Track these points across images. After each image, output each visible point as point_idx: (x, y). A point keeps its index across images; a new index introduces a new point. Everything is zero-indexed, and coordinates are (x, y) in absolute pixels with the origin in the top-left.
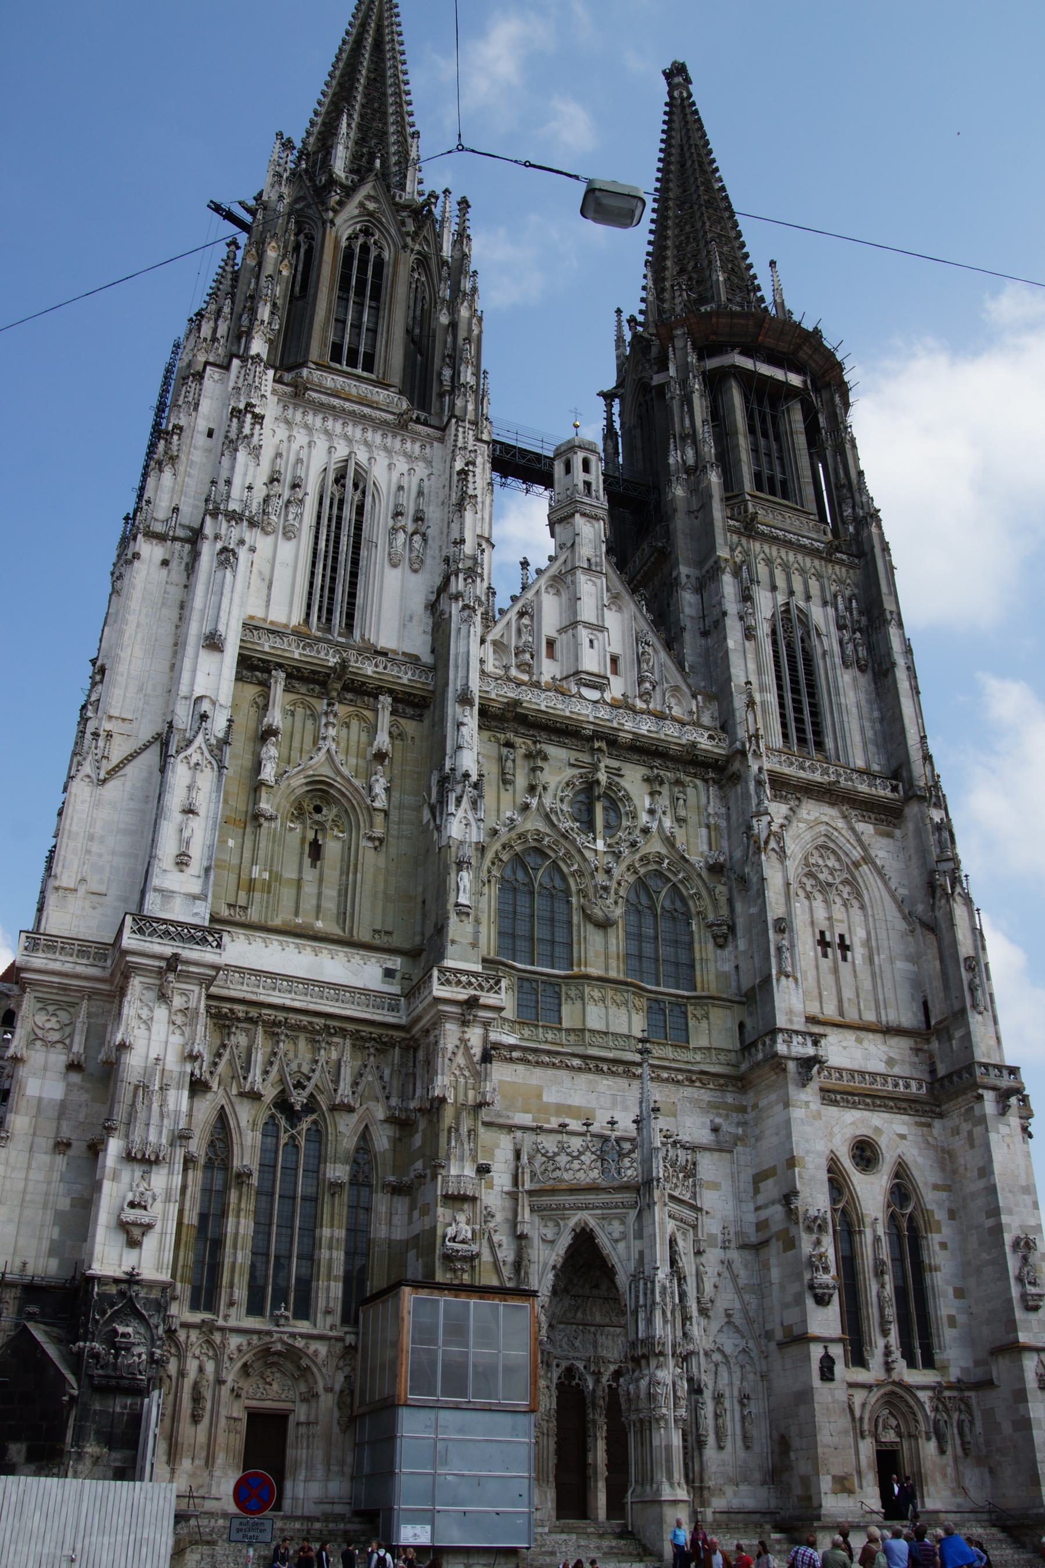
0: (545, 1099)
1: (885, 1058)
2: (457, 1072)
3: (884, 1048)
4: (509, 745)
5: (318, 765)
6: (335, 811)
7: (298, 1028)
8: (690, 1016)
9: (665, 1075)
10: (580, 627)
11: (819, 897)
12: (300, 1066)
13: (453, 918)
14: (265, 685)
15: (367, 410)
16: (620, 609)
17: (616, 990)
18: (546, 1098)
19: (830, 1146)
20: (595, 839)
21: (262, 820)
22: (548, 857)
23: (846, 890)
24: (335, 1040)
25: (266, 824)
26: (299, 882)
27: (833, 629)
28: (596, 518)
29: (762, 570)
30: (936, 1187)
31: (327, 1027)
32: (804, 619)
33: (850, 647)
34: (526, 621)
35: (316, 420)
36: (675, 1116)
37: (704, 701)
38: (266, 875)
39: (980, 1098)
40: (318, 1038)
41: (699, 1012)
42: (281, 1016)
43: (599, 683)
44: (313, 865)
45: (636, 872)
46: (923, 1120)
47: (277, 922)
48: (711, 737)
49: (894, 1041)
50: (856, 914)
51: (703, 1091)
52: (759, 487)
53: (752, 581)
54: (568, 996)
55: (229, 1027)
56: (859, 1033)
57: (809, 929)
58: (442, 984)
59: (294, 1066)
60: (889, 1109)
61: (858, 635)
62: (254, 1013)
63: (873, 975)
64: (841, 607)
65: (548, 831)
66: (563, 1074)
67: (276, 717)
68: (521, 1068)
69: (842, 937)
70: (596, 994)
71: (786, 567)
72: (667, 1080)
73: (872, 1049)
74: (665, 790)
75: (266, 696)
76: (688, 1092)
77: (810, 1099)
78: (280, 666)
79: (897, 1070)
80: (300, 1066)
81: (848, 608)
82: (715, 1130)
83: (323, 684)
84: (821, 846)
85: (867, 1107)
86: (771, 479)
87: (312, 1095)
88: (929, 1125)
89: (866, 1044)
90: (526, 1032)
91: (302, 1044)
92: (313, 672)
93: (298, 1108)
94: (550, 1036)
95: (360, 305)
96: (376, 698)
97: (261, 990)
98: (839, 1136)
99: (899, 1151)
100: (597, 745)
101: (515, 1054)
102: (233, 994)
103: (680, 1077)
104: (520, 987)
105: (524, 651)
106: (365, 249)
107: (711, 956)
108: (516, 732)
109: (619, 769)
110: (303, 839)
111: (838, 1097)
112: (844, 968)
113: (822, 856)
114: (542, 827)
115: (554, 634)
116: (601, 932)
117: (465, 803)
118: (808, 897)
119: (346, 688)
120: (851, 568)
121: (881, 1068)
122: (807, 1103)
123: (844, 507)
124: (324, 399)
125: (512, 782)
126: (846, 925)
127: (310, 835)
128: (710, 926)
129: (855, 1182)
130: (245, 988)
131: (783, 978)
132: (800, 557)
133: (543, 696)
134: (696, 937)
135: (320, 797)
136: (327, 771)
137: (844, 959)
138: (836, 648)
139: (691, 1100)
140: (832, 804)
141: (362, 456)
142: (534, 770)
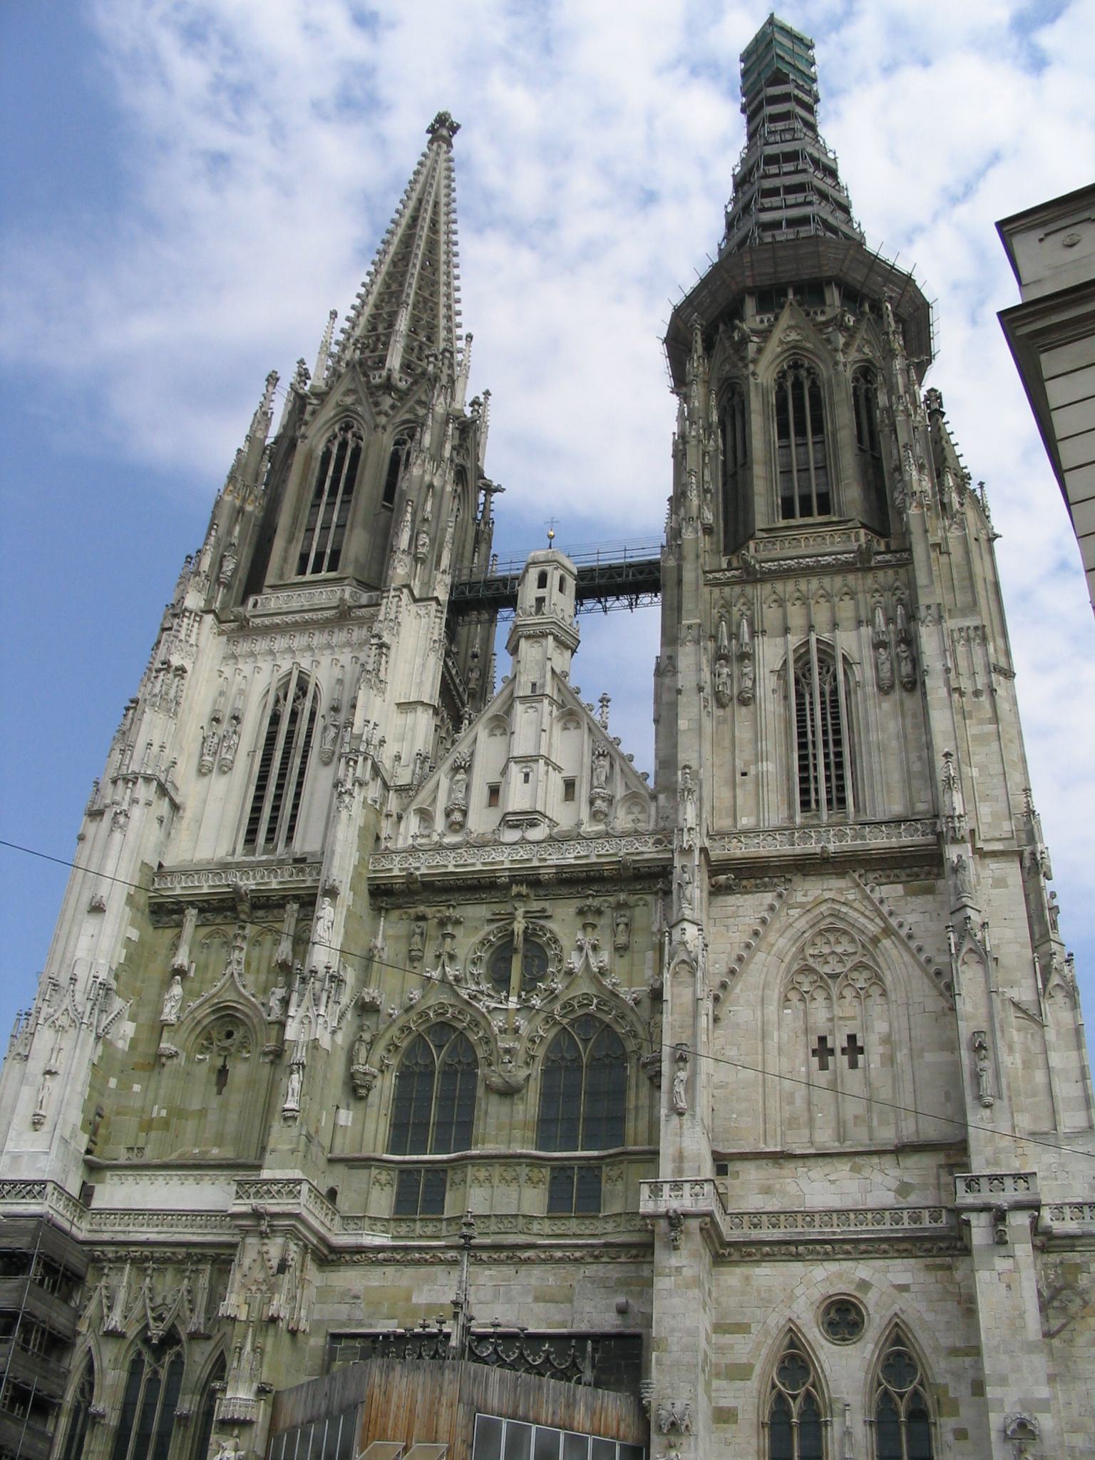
0: (414, 1300)
1: (894, 1184)
2: (254, 1288)
3: (897, 1172)
4: (422, 918)
5: (216, 989)
6: (242, 1032)
7: (167, 1261)
8: (604, 1178)
9: (559, 1254)
10: (512, 765)
11: (820, 996)
12: (165, 1297)
13: (277, 1125)
14: (179, 925)
15: (307, 616)
16: (578, 726)
17: (506, 1165)
18: (415, 1300)
19: (788, 1313)
20: (507, 999)
21: (164, 1060)
22: (455, 1029)
23: (861, 980)
24: (201, 1267)
25: (169, 1063)
26: (203, 1113)
27: (868, 653)
28: (544, 635)
29: (771, 615)
30: (954, 1352)
31: (189, 1255)
32: (827, 653)
33: (887, 666)
34: (461, 776)
35: (262, 645)
36: (571, 1301)
37: (667, 798)
38: (164, 1113)
39: (968, 1223)
40: (184, 1267)
41: (614, 1173)
42: (146, 1251)
43: (528, 819)
44: (220, 1092)
45: (556, 1023)
46: (938, 1261)
47: (173, 1157)
48: (658, 842)
49: (911, 1161)
50: (876, 1005)
51: (611, 1266)
52: (788, 512)
53: (753, 634)
54: (453, 1183)
55: (102, 1269)
56: (858, 1159)
57: (802, 1038)
58: (240, 1197)
59: (159, 1300)
60: (884, 1255)
61: (902, 646)
62: (122, 1251)
63: (895, 1078)
64: (880, 618)
65: (452, 1002)
66: (438, 1270)
67: (182, 958)
68: (390, 1270)
69: (852, 1038)
70: (482, 1174)
71: (804, 600)
72: (560, 1259)
73: (877, 1177)
74: (603, 921)
75: (179, 936)
76: (592, 1270)
77: (685, 1262)
78: (192, 904)
79: (913, 1199)
80: (165, 1297)
81: (890, 620)
82: (622, 1311)
83: (233, 909)
84: (827, 930)
85: (848, 1256)
86: (805, 500)
87: (174, 1326)
88: (949, 1268)
89: (866, 1172)
90: (403, 1229)
91: (169, 1276)
92: (221, 900)
93: (155, 1341)
94: (430, 1230)
95: (331, 504)
96: (282, 906)
97: (131, 1228)
98: (802, 1300)
99: (896, 1308)
100: (515, 890)
101: (381, 1256)
102: (106, 1237)
103: (578, 1254)
104: (401, 1184)
105: (452, 810)
106: (343, 445)
107: (647, 1102)
108: (430, 904)
109: (543, 910)
110: (211, 1068)
111: (801, 1249)
112: (853, 1080)
113: (828, 943)
114: (445, 998)
115: (495, 778)
116: (508, 1101)
117: (307, 1001)
118: (802, 1000)
119: (255, 907)
120: (900, 566)
121: (889, 1199)
122: (678, 1270)
123: (896, 495)
124: (267, 621)
125: (420, 959)
126: (858, 1022)
127: (219, 1063)
128: (645, 1065)
129: (822, 1357)
130: (117, 1228)
131: (675, 1119)
132: (826, 581)
133: (453, 855)
134: (633, 1082)
135: (230, 1022)
136: (230, 995)
137: (853, 1065)
138: (870, 674)
139: (593, 1280)
140: (841, 874)
141: (305, 663)
142: (445, 936)
